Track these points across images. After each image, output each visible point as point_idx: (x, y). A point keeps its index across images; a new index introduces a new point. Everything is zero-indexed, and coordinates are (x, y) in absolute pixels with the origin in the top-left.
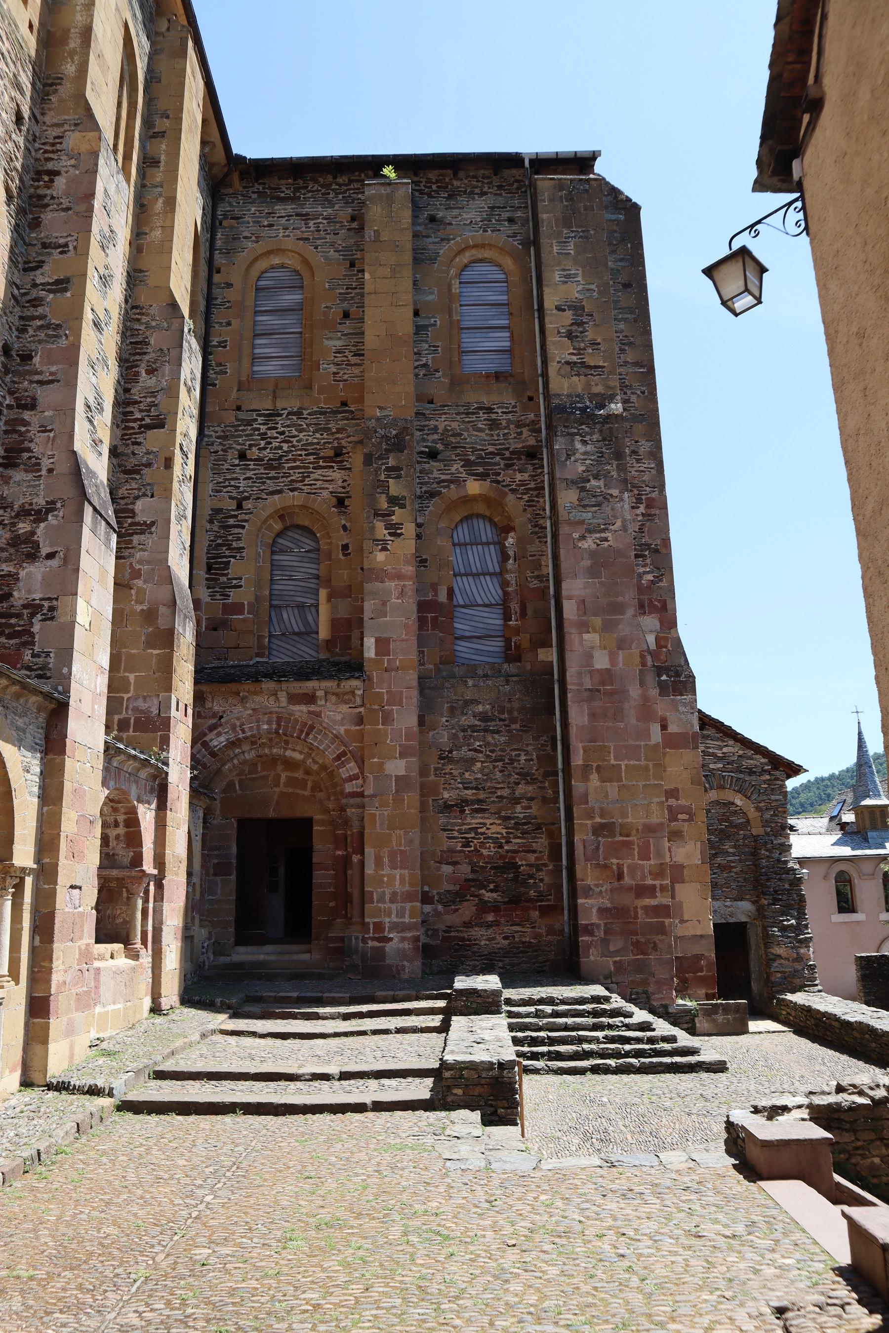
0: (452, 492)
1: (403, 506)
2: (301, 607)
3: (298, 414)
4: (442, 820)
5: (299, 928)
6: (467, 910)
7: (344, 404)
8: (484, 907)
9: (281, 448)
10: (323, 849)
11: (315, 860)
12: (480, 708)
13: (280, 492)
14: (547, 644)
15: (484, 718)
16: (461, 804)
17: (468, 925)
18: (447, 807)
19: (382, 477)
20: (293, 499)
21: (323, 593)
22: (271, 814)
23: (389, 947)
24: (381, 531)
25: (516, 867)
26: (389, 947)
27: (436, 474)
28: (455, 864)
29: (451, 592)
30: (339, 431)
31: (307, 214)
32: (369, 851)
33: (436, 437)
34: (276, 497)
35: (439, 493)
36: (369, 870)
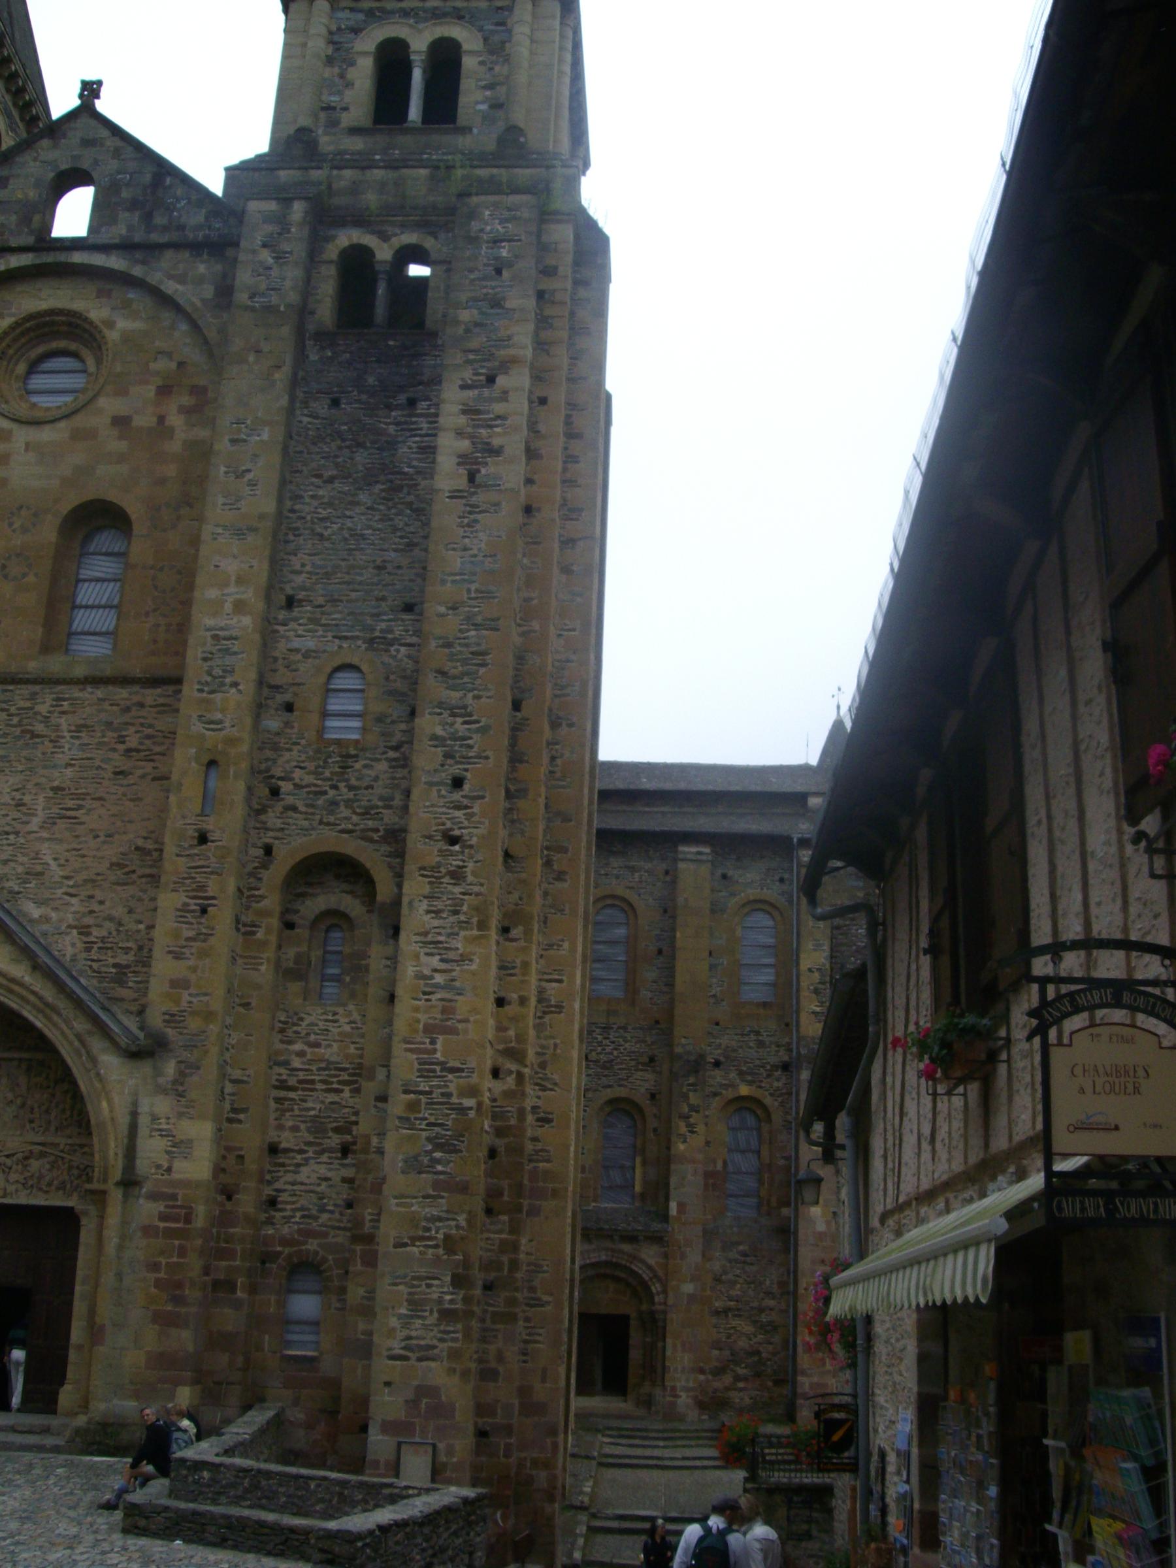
0: (730, 1094)
1: (697, 1112)
2: (622, 1167)
3: (625, 1028)
4: (714, 1320)
5: (616, 1384)
6: (727, 1379)
7: (657, 1022)
8: (738, 1378)
9: (611, 1053)
10: (636, 1337)
11: (631, 1342)
12: (741, 1248)
13: (610, 1086)
14: (788, 1204)
15: (745, 1254)
16: (726, 1311)
17: (727, 1389)
18: (717, 1313)
19: (685, 1090)
20: (621, 1092)
21: (638, 1160)
22: (603, 1311)
23: (679, 1401)
24: (683, 1129)
25: (758, 1353)
26: (679, 1401)
27: (719, 1079)
28: (720, 1349)
29: (725, 1163)
30: (653, 1043)
31: (633, 867)
32: (669, 1341)
33: (719, 1051)
34: (609, 1090)
35: (720, 1094)
36: (669, 1353)
